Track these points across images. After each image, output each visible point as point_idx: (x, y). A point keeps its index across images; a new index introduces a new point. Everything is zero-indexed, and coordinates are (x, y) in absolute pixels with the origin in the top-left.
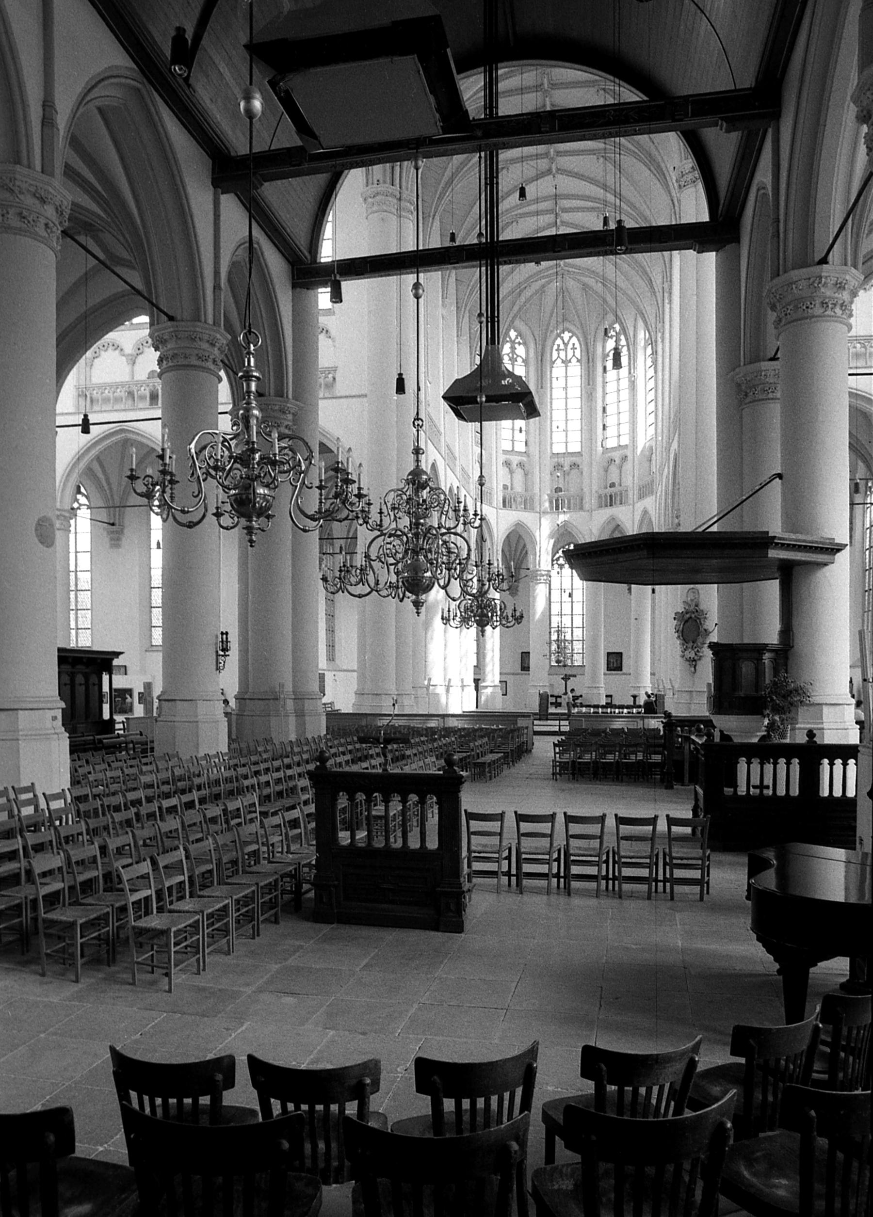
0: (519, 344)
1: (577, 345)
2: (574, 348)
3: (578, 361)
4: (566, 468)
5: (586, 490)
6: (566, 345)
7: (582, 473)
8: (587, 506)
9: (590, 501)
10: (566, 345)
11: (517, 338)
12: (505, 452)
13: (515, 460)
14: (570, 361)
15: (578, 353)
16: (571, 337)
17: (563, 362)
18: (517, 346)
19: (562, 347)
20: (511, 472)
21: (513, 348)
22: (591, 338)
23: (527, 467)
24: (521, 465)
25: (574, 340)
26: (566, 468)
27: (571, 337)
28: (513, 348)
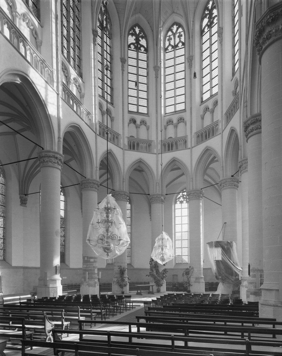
0: (142, 37)
1: (182, 33)
2: (180, 36)
3: (183, 44)
4: (175, 121)
5: (188, 134)
6: (174, 34)
7: (186, 124)
8: (189, 145)
9: (191, 141)
10: (174, 34)
11: (140, 33)
12: (130, 112)
13: (138, 119)
14: (177, 46)
15: (183, 39)
16: (177, 29)
17: (173, 47)
18: (140, 39)
19: (172, 37)
20: (137, 127)
21: (137, 40)
22: (191, 19)
23: (148, 124)
24: (143, 122)
25: (180, 30)
26: (175, 121)
27: (177, 29)
28: (137, 40)
